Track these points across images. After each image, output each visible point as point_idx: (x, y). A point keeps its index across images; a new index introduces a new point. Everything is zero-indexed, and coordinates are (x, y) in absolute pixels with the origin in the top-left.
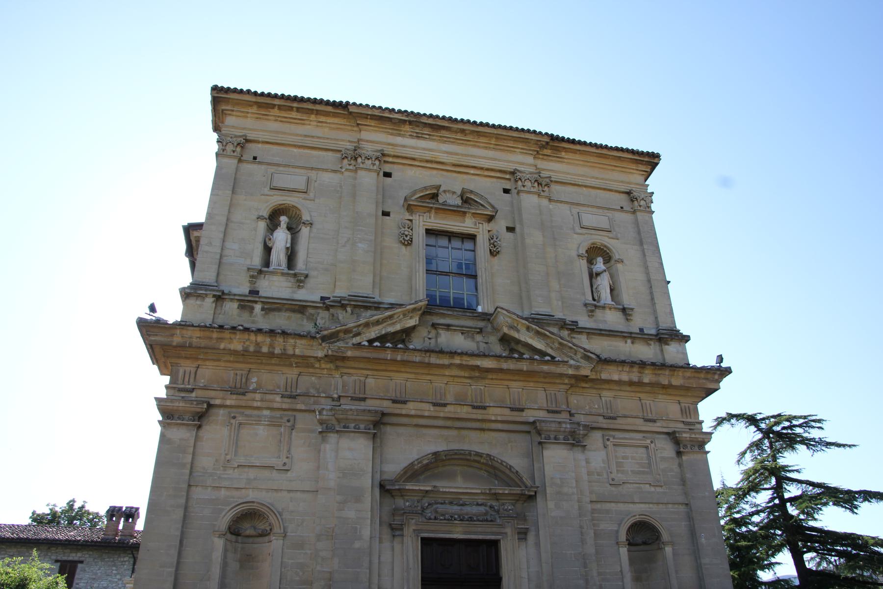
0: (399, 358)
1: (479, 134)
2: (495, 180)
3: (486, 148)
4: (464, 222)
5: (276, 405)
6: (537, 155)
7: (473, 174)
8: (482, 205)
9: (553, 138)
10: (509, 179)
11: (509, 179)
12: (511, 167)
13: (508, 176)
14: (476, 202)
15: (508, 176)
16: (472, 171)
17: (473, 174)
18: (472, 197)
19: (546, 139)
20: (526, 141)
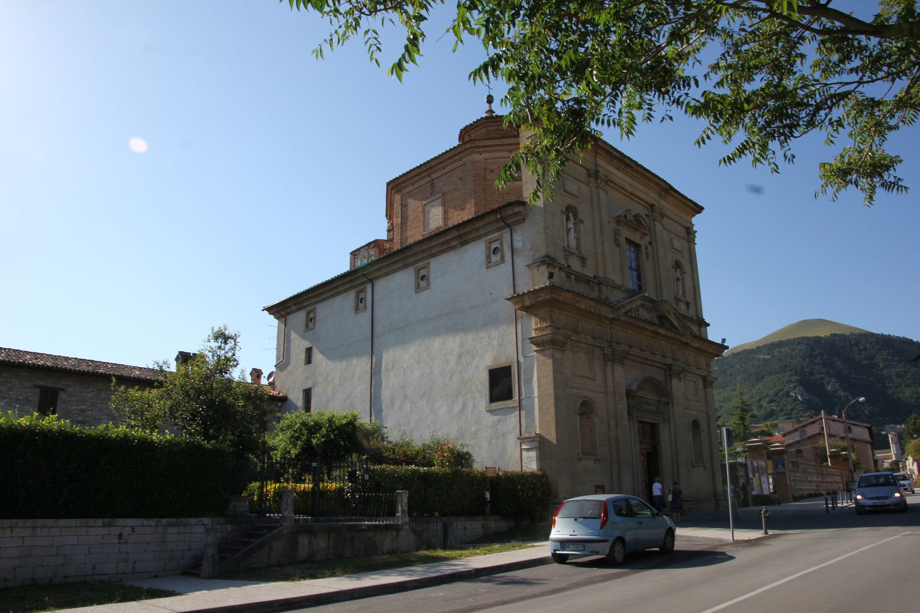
0: (637, 324)
1: (642, 175)
2: (642, 207)
3: (642, 185)
4: (636, 235)
5: (589, 342)
6: (660, 196)
7: (636, 201)
8: (643, 226)
9: (671, 188)
10: (648, 208)
11: (648, 208)
12: (653, 202)
13: (648, 206)
14: (641, 223)
15: (648, 206)
16: (636, 199)
17: (636, 201)
18: (641, 220)
19: (667, 187)
20: (659, 185)
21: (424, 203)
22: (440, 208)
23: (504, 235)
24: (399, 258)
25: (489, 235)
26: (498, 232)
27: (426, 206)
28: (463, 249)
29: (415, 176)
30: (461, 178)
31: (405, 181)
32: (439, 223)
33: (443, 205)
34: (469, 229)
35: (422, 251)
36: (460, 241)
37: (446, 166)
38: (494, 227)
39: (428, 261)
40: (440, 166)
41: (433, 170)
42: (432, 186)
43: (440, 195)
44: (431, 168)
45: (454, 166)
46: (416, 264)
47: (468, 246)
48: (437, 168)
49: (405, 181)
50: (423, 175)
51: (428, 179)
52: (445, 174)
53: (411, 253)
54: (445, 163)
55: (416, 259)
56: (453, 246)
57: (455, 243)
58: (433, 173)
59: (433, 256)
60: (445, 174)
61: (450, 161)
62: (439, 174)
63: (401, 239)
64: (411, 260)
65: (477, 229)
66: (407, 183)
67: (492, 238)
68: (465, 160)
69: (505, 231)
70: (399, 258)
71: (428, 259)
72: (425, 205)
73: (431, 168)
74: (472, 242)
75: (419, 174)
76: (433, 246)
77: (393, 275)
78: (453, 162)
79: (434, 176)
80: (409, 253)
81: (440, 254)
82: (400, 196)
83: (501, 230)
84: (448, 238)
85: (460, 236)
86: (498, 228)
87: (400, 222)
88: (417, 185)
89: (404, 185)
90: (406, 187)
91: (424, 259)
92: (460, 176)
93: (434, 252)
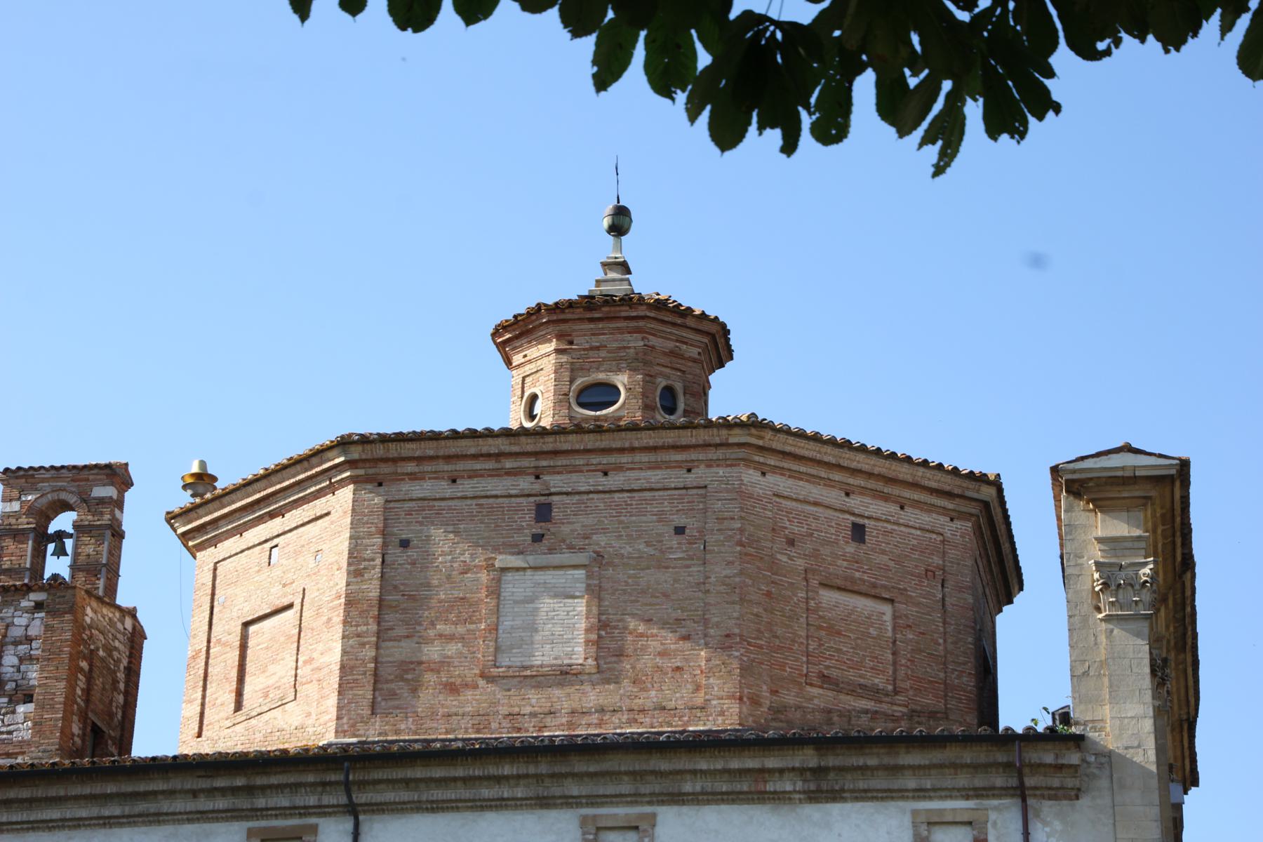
21: (502, 560)
22: (581, 606)
23: (993, 816)
24: (532, 770)
25: (931, 798)
26: (967, 798)
27: (509, 576)
28: (813, 812)
29: (475, 457)
30: (680, 530)
31: (420, 460)
32: (570, 655)
33: (595, 592)
34: (872, 762)
35: (636, 775)
36: (813, 787)
37: (619, 468)
38: (962, 780)
39: (648, 809)
40: (595, 459)
41: (561, 461)
42: (543, 513)
43: (582, 558)
44: (556, 453)
45: (655, 477)
46: (592, 805)
47: (835, 809)
48: (579, 461)
49: (420, 460)
50: (509, 464)
51: (525, 483)
52: (610, 492)
53: (593, 768)
54: (624, 459)
55: (601, 791)
56: (775, 792)
57: (789, 787)
58: (553, 470)
59: (677, 799)
60: (610, 492)
61: (644, 457)
62: (583, 482)
63: (376, 660)
64: (574, 789)
65: (896, 770)
66: (427, 467)
67: (941, 811)
68: (701, 474)
69: (995, 802)
70: (532, 770)
71: (650, 803)
72: (504, 570)
73: (556, 453)
74: (857, 799)
75: (499, 456)
76: (694, 772)
77: (469, 816)
78: (655, 466)
79: (556, 482)
80: (580, 766)
81: (708, 802)
82: (378, 500)
83: (978, 797)
84: (772, 762)
85: (819, 772)
86: (975, 789)
87: (375, 594)
88: (466, 487)
89: (411, 467)
90: (413, 477)
91: (635, 798)
92: (680, 520)
93: (688, 787)
